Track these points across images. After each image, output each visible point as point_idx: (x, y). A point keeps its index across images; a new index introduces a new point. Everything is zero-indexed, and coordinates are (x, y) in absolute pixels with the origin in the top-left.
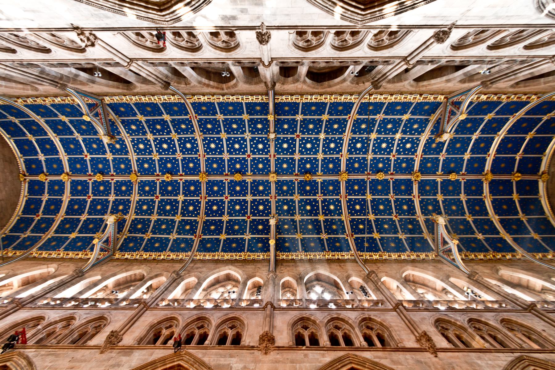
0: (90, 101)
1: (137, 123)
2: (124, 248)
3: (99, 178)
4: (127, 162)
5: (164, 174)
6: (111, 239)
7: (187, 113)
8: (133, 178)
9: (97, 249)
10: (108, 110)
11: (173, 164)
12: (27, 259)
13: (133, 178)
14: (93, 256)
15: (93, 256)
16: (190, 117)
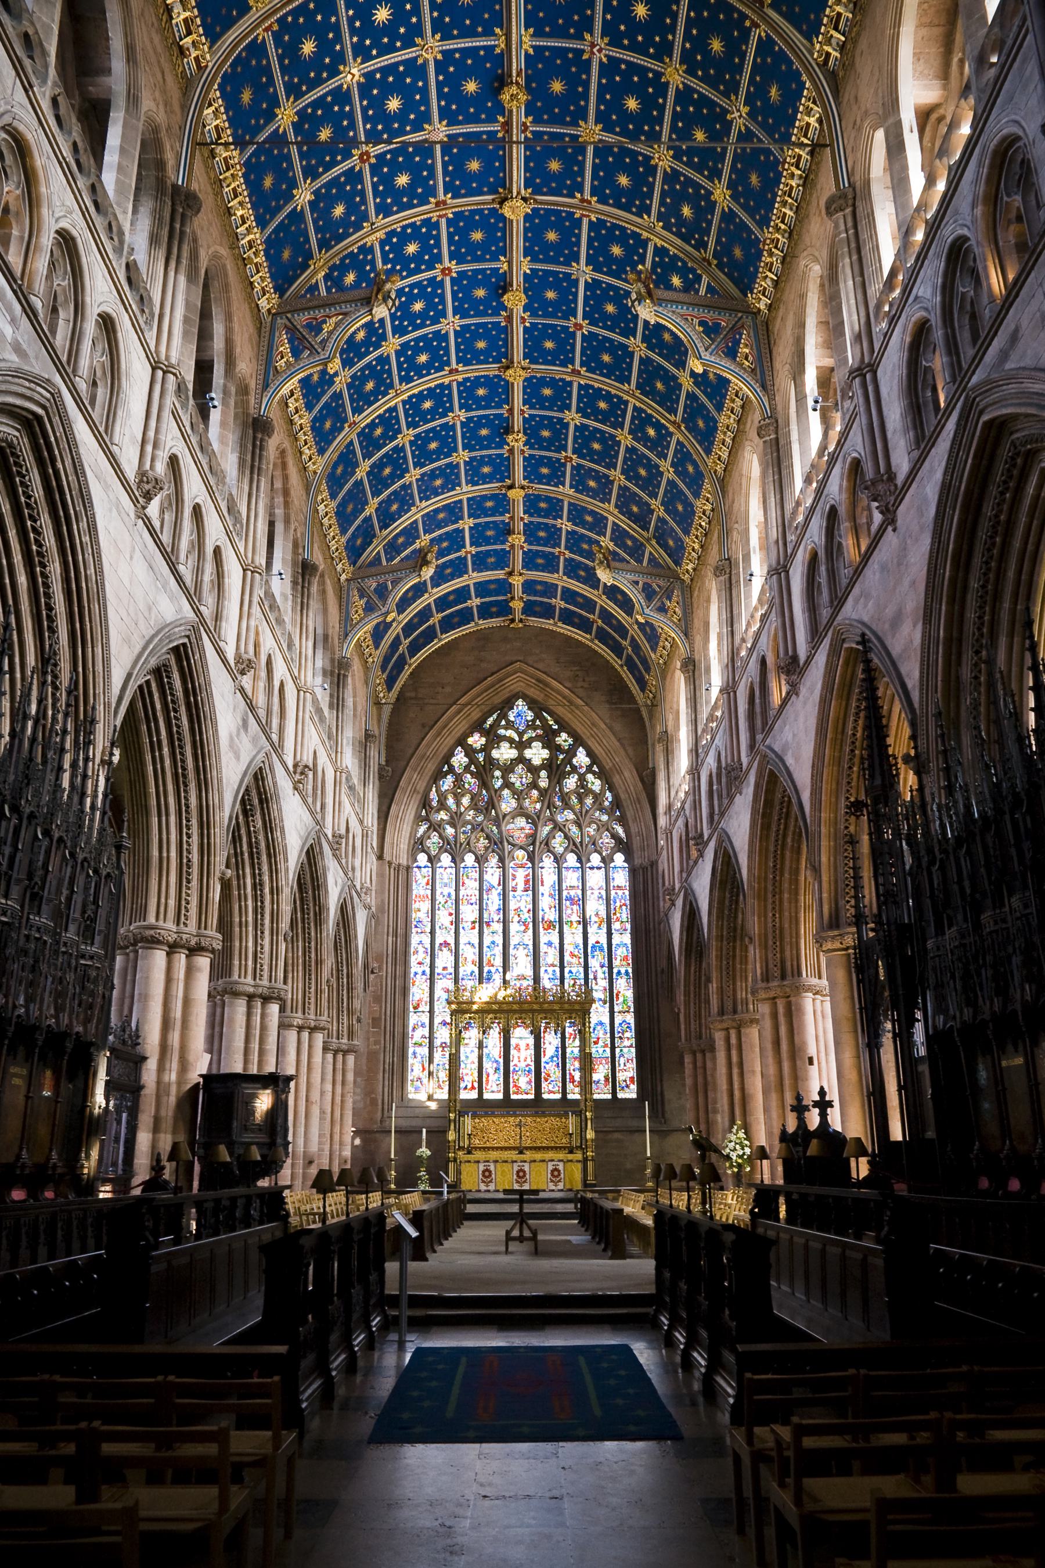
0: (285, 348)
1: (322, 202)
2: (744, 280)
3: (516, 300)
4: (462, 224)
5: (500, 108)
6: (709, 316)
7: (257, 49)
8: (515, 212)
9: (724, 367)
10: (297, 296)
11: (466, 73)
12: (723, 483)
13: (515, 212)
14: (741, 385)
15: (741, 385)
16: (266, 30)
